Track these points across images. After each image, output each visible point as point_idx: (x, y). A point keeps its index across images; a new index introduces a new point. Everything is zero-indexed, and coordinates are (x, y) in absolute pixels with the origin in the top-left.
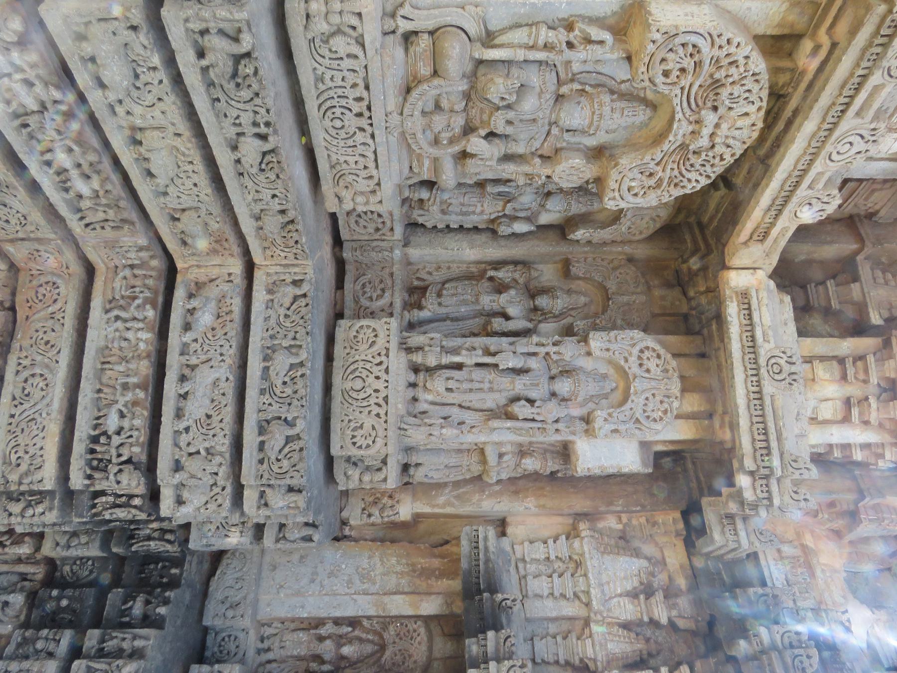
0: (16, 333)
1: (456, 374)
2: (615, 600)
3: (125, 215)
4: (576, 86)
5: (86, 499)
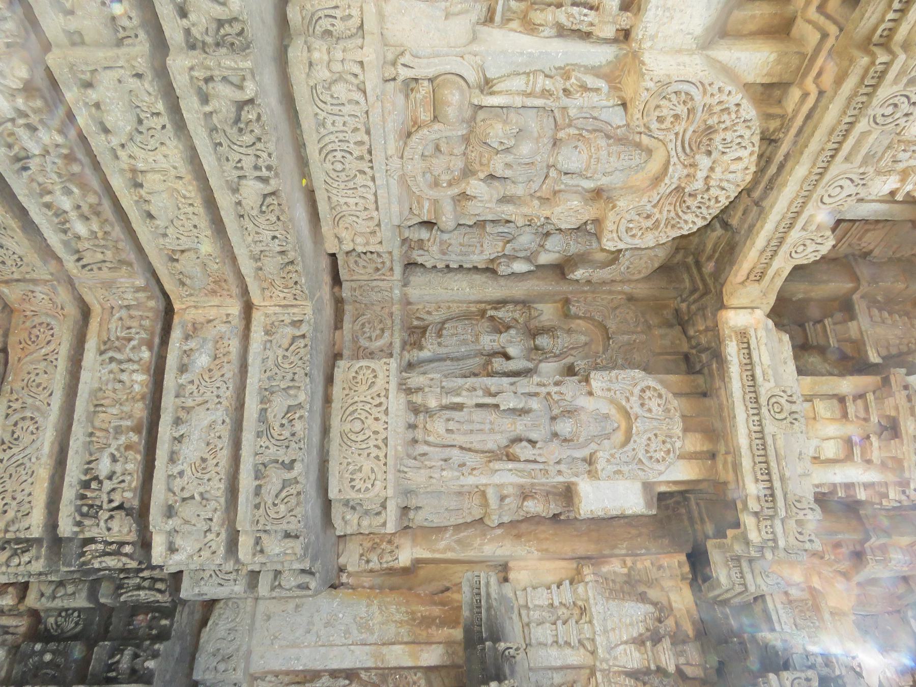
0: (7, 375)
1: (456, 415)
2: (622, 647)
3: (124, 256)
4: (572, 131)
5: (74, 548)
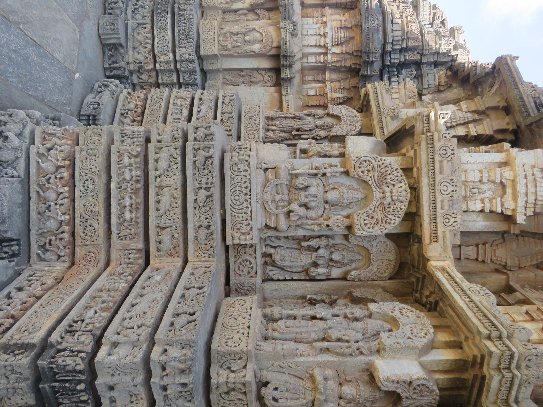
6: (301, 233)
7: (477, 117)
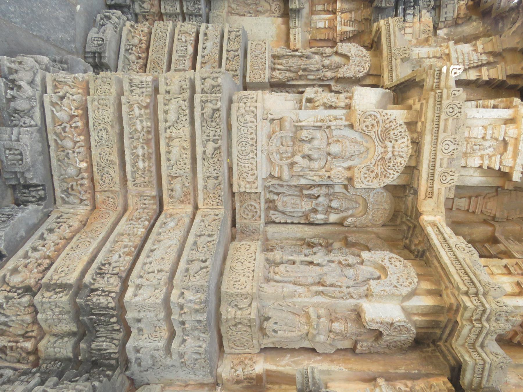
5: (87, 291)
6: (303, 182)
7: (492, 59)
